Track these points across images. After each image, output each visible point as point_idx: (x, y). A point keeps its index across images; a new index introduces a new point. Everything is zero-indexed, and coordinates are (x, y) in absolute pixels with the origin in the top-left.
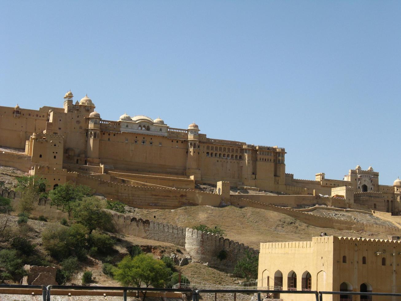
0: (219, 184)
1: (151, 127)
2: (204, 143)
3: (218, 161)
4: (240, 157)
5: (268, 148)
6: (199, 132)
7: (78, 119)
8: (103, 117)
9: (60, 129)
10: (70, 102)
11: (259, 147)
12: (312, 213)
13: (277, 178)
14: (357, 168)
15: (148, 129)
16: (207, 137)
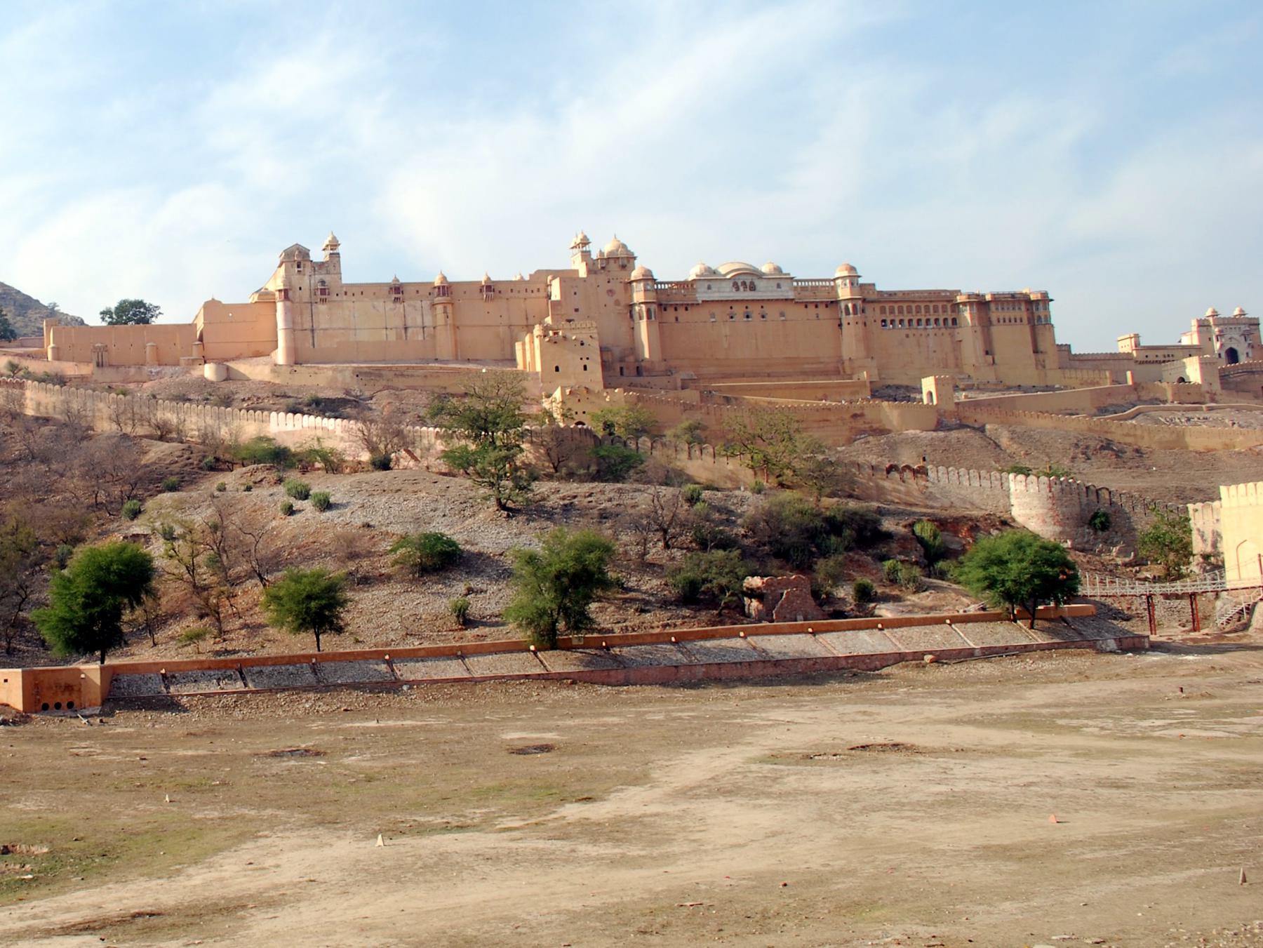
0: (928, 384)
1: (757, 282)
2: (872, 302)
3: (907, 336)
4: (954, 321)
5: (1013, 296)
6: (861, 281)
7: (609, 286)
8: (659, 277)
9: (577, 310)
10: (586, 255)
11: (993, 295)
12: (1134, 422)
13: (1041, 357)
14: (1209, 313)
15: (753, 288)
16: (878, 288)
